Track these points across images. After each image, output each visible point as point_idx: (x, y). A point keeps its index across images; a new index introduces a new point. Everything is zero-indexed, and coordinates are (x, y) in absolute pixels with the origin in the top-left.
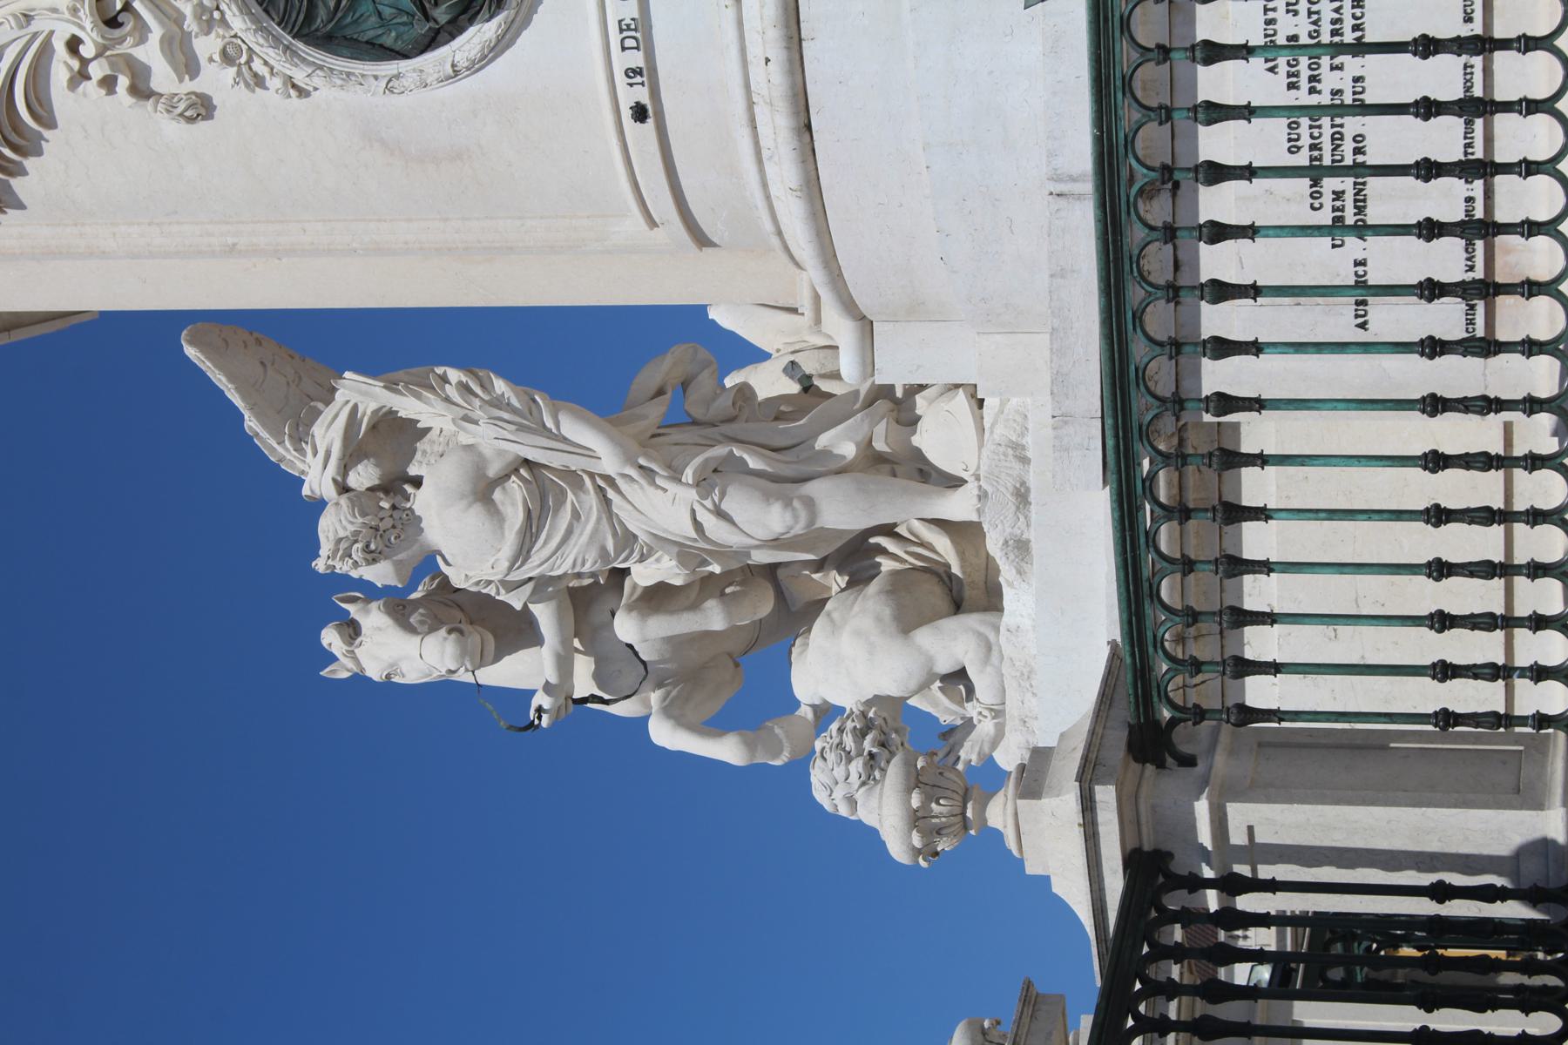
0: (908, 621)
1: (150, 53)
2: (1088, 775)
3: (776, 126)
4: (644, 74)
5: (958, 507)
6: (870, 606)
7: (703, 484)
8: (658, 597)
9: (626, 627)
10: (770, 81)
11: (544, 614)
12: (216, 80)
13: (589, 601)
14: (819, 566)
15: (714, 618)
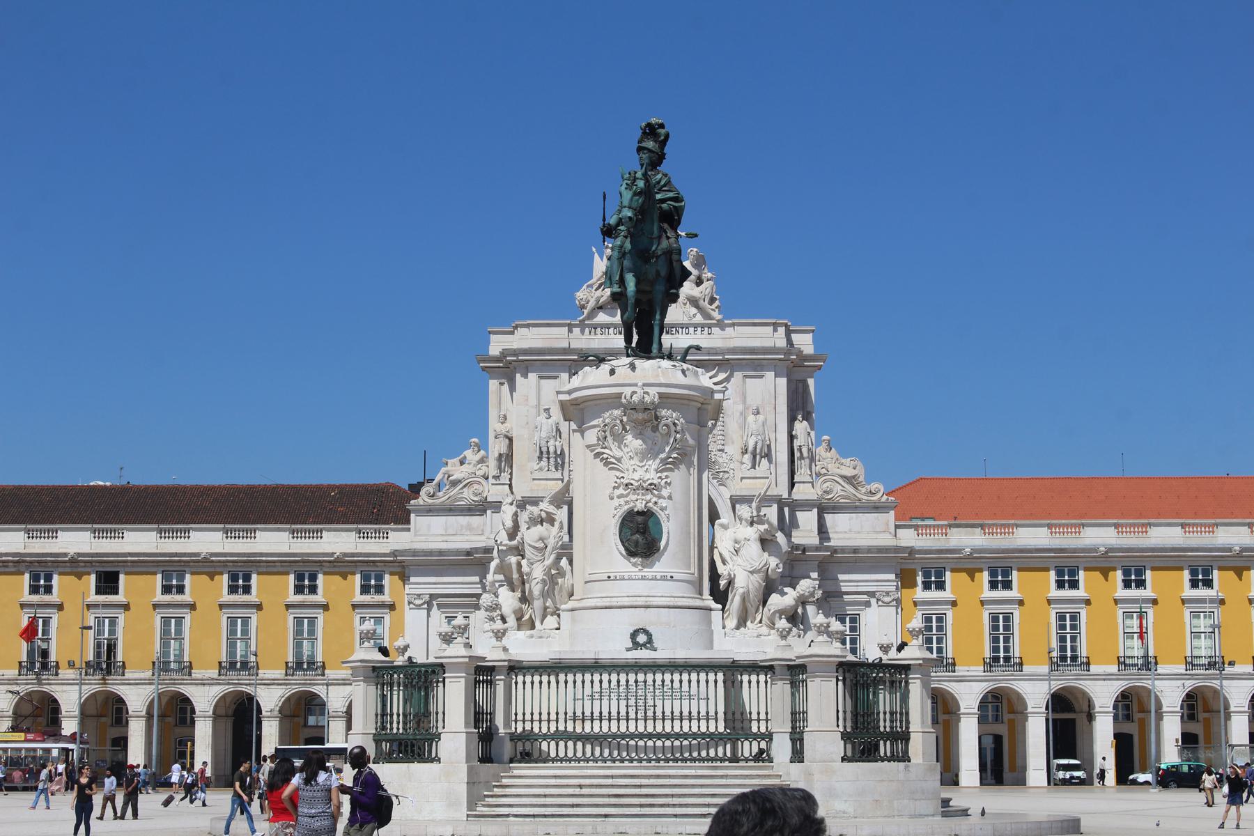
0: (515, 612)
1: (621, 491)
2: (509, 661)
3: (606, 602)
4: (616, 579)
5: (537, 624)
6: (517, 604)
7: (543, 580)
8: (519, 565)
9: (513, 560)
10: (614, 602)
11: (515, 543)
12: (616, 502)
13: (519, 551)
14: (523, 592)
15: (515, 576)
